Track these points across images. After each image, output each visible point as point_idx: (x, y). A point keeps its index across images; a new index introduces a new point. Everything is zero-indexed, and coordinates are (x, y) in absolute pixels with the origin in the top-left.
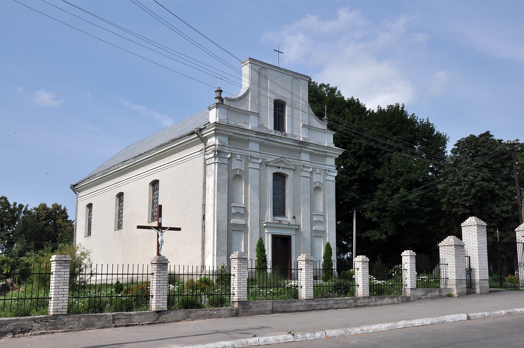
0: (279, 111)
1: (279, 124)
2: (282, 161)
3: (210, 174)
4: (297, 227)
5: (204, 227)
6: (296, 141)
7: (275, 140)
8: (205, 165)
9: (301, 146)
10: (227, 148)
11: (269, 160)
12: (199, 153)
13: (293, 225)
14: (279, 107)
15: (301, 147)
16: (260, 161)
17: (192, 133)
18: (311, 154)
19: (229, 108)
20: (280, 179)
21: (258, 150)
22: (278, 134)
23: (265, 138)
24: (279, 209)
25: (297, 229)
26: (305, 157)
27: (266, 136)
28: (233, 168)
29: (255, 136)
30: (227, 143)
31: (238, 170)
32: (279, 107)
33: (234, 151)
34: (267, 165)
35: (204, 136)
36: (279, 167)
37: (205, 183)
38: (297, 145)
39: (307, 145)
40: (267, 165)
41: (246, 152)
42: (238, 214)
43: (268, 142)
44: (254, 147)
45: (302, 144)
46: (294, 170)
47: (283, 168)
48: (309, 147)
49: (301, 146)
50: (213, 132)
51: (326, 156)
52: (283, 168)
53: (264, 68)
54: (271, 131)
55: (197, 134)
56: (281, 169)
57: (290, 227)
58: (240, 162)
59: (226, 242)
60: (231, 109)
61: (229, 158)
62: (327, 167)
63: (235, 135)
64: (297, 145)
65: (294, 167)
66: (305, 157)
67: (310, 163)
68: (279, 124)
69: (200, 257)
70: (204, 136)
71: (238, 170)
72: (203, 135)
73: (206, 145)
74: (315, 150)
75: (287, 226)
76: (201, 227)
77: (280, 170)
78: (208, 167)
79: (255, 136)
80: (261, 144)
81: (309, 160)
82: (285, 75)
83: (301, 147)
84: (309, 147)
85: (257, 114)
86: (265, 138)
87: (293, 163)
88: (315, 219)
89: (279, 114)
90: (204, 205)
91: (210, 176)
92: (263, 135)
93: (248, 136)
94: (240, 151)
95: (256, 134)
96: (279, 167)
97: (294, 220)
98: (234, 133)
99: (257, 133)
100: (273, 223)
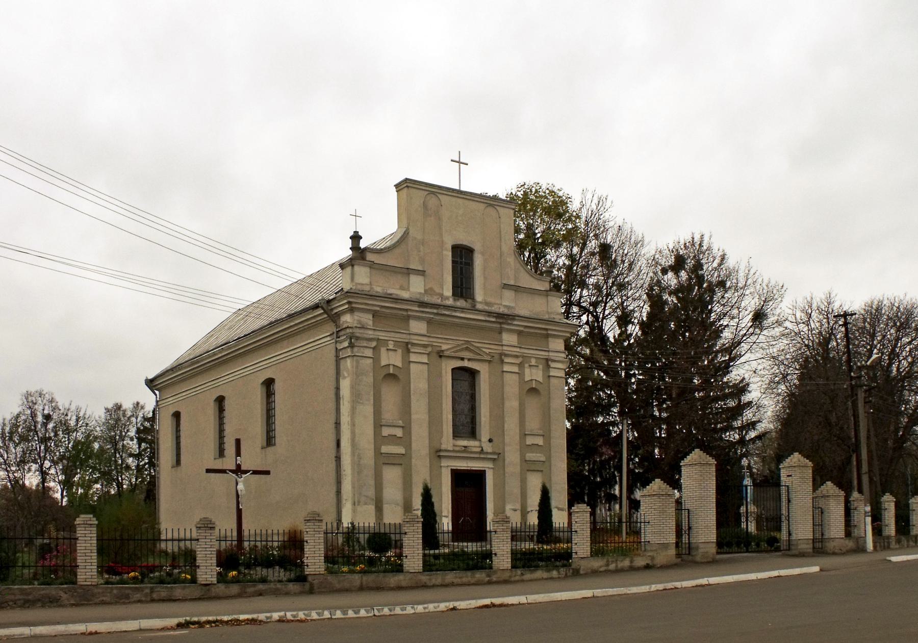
0: (461, 263)
1: (463, 285)
2: (467, 349)
3: (346, 375)
4: (496, 457)
5: (338, 458)
6: (489, 314)
7: (454, 314)
8: (338, 360)
9: (501, 321)
10: (370, 332)
11: (444, 347)
12: (328, 339)
13: (487, 453)
14: (463, 257)
15: (501, 323)
16: (429, 349)
17: (316, 307)
18: (520, 333)
19: (372, 266)
20: (466, 377)
21: (424, 332)
22: (461, 303)
23: (435, 311)
24: (467, 426)
25: (498, 458)
26: (509, 339)
28: (383, 363)
29: (417, 309)
30: (371, 323)
31: (391, 367)
32: (463, 257)
33: (382, 335)
34: (441, 356)
35: (335, 311)
36: (462, 359)
37: (338, 389)
38: (494, 320)
40: (441, 356)
41: (404, 336)
42: (393, 440)
43: (443, 318)
45: (502, 318)
47: (469, 360)
48: (515, 323)
49: (501, 321)
50: (347, 306)
51: (547, 336)
52: (469, 360)
53: (433, 193)
54: (447, 298)
55: (323, 309)
56: (466, 361)
57: (482, 456)
59: (372, 482)
60: (375, 266)
61: (374, 348)
62: (551, 354)
64: (494, 320)
65: (488, 358)
66: (509, 339)
67: (518, 350)
68: (463, 285)
69: (335, 506)
70: (335, 311)
71: (391, 367)
72: (332, 310)
73: (337, 326)
76: (334, 459)
77: (466, 364)
78: (342, 362)
79: (417, 309)
80: (430, 322)
81: (516, 344)
82: (471, 203)
83: (501, 323)
84: (515, 323)
86: (435, 311)
87: (487, 351)
88: (530, 441)
89: (461, 268)
90: (338, 424)
91: (345, 378)
92: (431, 308)
93: (407, 310)
94: (393, 334)
95: (419, 306)
96: (462, 359)
97: (491, 444)
99: (422, 304)
100: (453, 451)
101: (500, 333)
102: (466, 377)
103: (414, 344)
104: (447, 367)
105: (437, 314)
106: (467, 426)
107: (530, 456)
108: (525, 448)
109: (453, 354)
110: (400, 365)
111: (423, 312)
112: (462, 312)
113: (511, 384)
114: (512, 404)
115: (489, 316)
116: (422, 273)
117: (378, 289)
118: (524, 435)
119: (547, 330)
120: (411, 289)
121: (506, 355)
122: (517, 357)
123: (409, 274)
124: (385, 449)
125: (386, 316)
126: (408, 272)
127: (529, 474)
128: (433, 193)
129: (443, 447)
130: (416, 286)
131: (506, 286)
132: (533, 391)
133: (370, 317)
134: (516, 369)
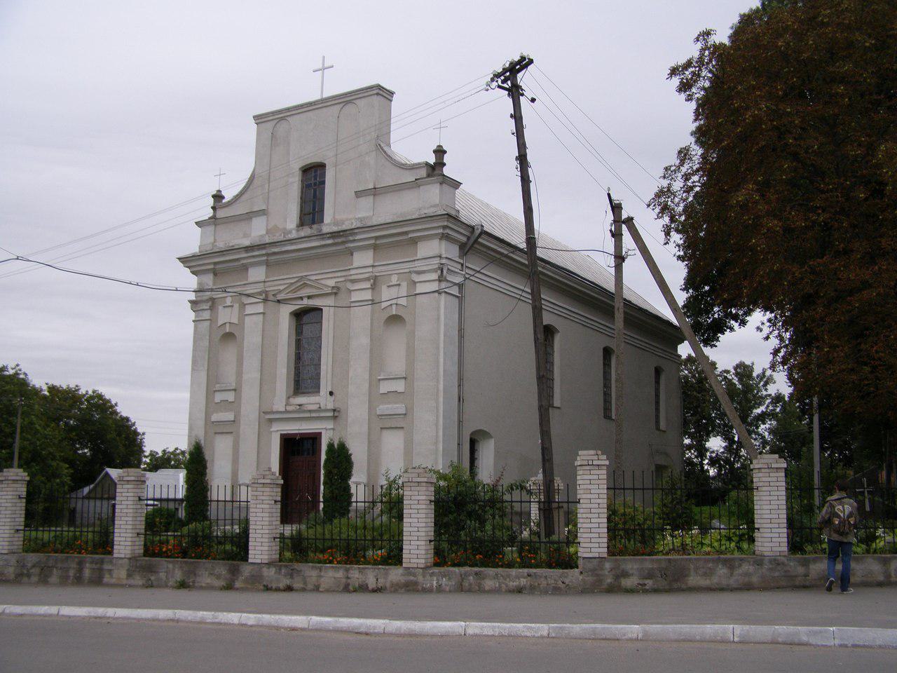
1: (312, 209)
2: (305, 285)
4: (331, 414)
11: (282, 288)
15: (343, 243)
18: (375, 247)
20: (306, 318)
23: (264, 252)
24: (304, 377)
27: (264, 248)
28: (220, 323)
32: (313, 175)
36: (301, 298)
38: (330, 241)
39: (351, 235)
44: (257, 274)
46: (336, 294)
47: (309, 297)
48: (358, 237)
51: (414, 242)
52: (309, 297)
54: (290, 232)
57: (322, 415)
58: (230, 308)
63: (217, 267)
64: (330, 241)
68: (312, 209)
71: (228, 325)
74: (377, 238)
75: (307, 415)
77: (306, 302)
80: (268, 264)
82: (324, 110)
84: (358, 237)
85: (261, 213)
86: (264, 252)
87: (331, 283)
88: (385, 387)
92: (259, 249)
96: (301, 298)
97: (333, 398)
98: (215, 264)
101: (352, 255)
102: (306, 318)
103: (248, 295)
104: (286, 312)
105: (268, 255)
106: (304, 377)
107: (384, 408)
108: (374, 397)
109: (290, 296)
110: (236, 321)
111: (253, 257)
112: (292, 244)
113: (361, 319)
114: (361, 341)
115: (323, 239)
116: (263, 212)
117: (221, 245)
118: (374, 382)
119: (406, 233)
120: (253, 235)
121: (353, 281)
122: (368, 279)
123: (251, 218)
124: (215, 417)
125: (226, 272)
126: (249, 216)
127: (386, 434)
128: (282, 119)
129: (275, 408)
130: (258, 231)
131: (359, 194)
132: (395, 319)
133: (211, 276)
134: (367, 295)
